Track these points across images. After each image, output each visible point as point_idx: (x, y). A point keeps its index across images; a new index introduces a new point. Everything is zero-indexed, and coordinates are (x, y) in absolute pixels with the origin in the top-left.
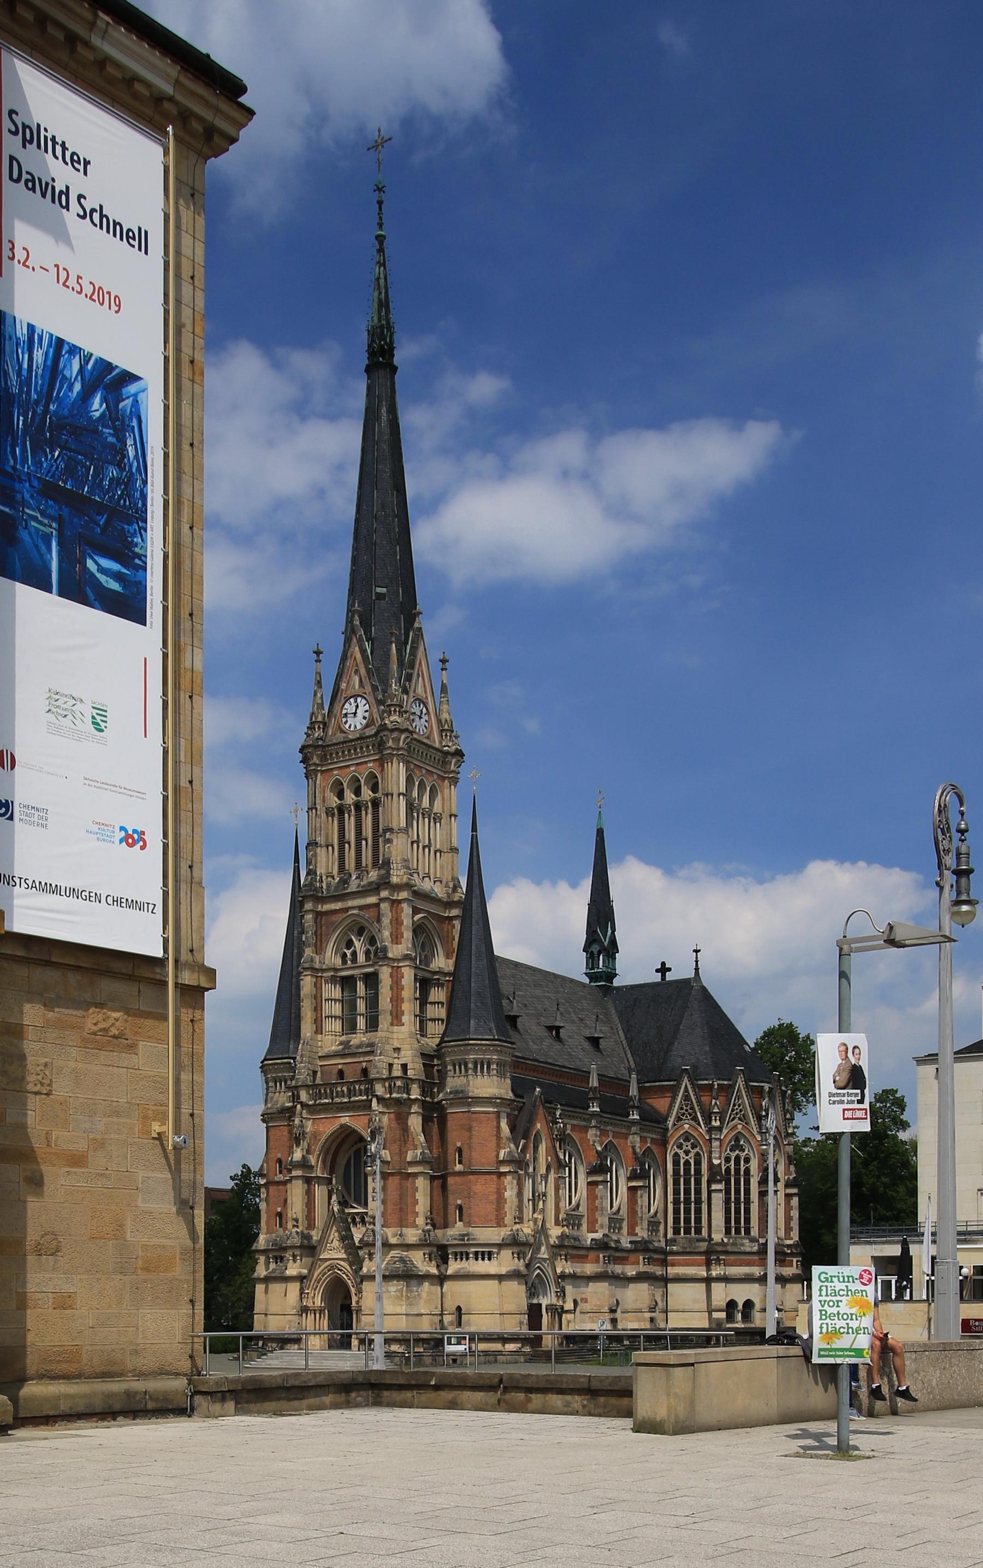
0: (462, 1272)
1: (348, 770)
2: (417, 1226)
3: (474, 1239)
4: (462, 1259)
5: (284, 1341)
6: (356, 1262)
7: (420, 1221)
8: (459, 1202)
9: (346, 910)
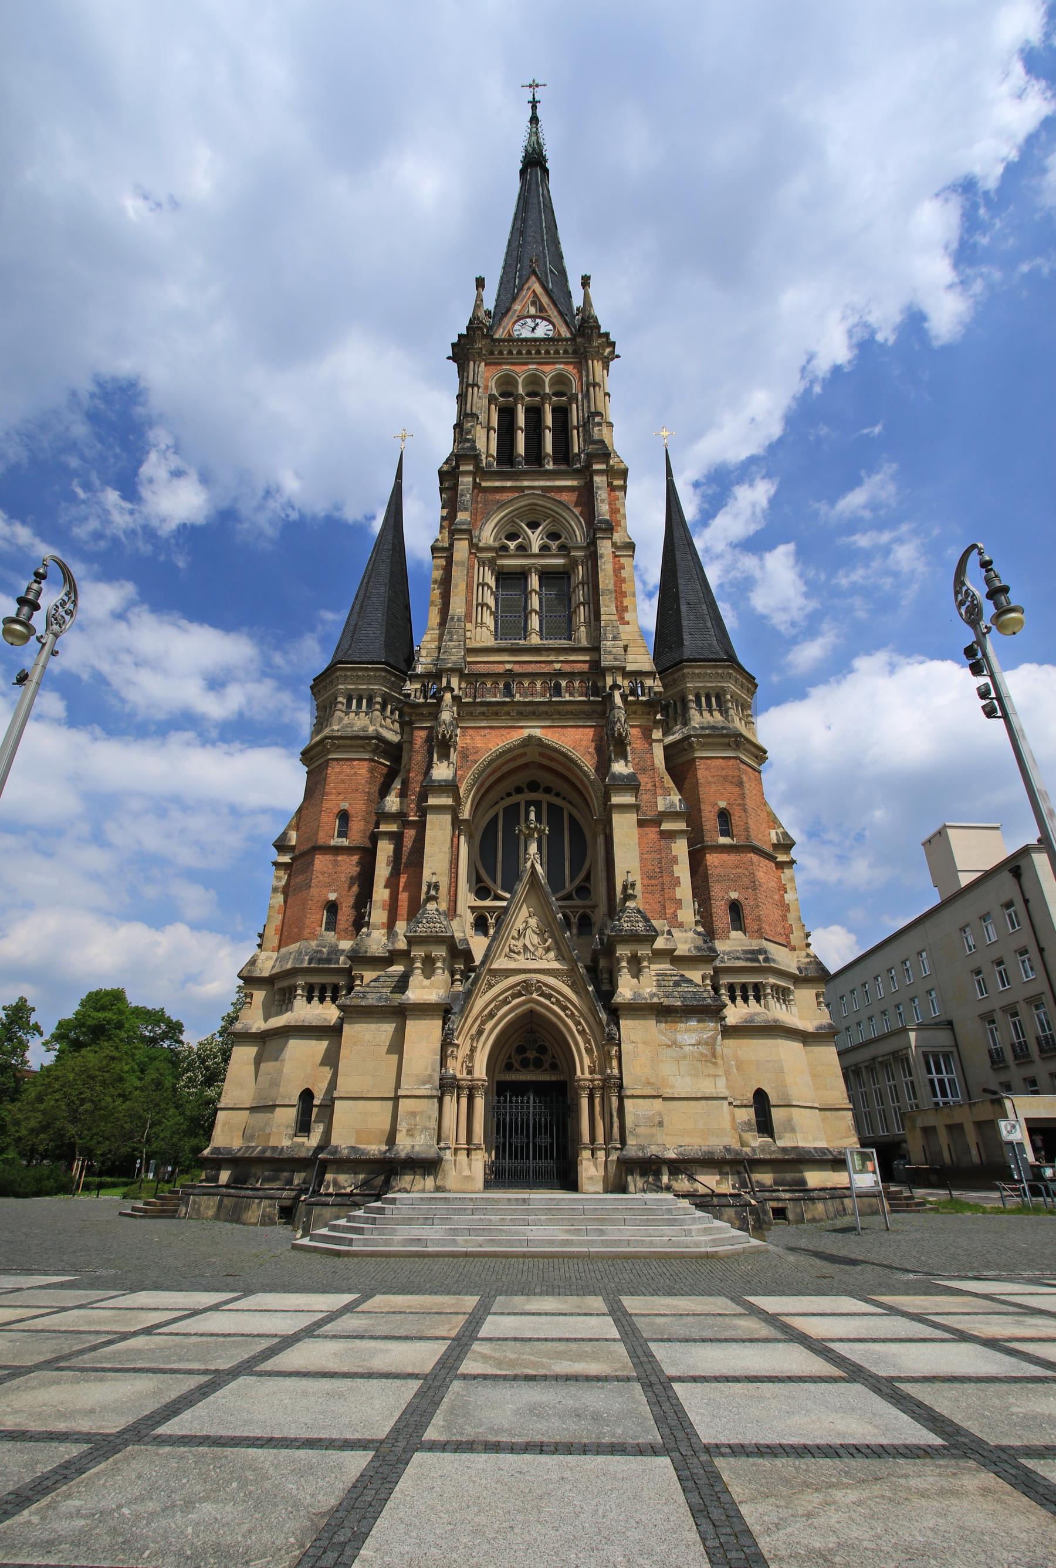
0: (759, 1021)
1: (526, 368)
2: (680, 925)
3: (774, 961)
4: (745, 999)
5: (384, 1172)
6: (598, 977)
7: (688, 914)
8: (734, 895)
9: (522, 489)
